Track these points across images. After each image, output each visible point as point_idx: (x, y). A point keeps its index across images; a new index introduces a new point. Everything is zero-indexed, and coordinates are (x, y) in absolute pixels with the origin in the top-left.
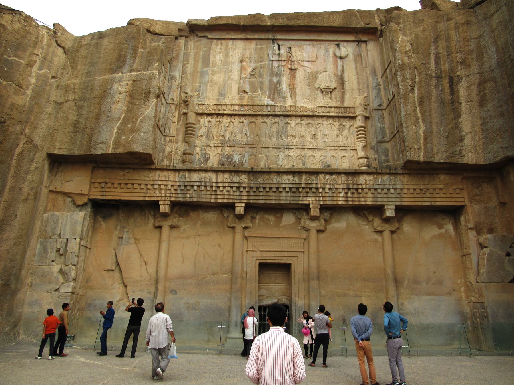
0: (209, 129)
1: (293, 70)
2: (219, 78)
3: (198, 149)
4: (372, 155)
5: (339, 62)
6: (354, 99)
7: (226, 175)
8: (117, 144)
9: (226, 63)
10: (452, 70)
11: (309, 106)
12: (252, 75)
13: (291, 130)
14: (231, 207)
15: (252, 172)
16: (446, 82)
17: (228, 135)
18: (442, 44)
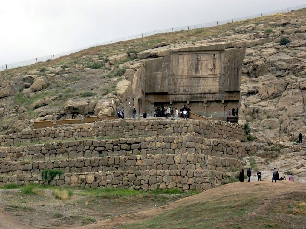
0: (180, 82)
1: (202, 63)
2: (182, 67)
3: (178, 88)
4: (221, 87)
5: (214, 60)
6: (218, 72)
7: (185, 95)
8: (160, 90)
9: (183, 62)
10: (238, 66)
11: (206, 74)
12: (190, 66)
13: (201, 81)
14: (186, 102)
15: (191, 94)
16: (236, 70)
17: (185, 83)
18: (236, 59)
